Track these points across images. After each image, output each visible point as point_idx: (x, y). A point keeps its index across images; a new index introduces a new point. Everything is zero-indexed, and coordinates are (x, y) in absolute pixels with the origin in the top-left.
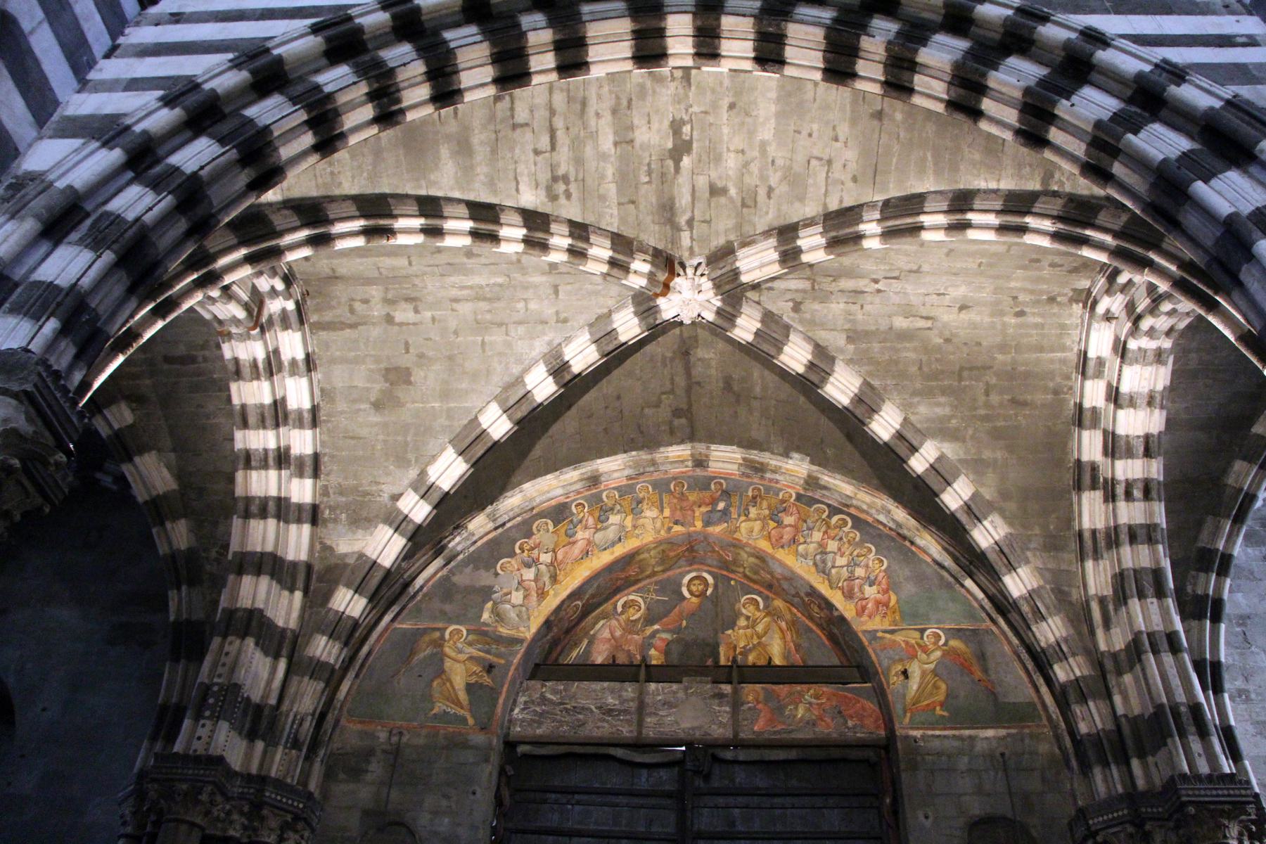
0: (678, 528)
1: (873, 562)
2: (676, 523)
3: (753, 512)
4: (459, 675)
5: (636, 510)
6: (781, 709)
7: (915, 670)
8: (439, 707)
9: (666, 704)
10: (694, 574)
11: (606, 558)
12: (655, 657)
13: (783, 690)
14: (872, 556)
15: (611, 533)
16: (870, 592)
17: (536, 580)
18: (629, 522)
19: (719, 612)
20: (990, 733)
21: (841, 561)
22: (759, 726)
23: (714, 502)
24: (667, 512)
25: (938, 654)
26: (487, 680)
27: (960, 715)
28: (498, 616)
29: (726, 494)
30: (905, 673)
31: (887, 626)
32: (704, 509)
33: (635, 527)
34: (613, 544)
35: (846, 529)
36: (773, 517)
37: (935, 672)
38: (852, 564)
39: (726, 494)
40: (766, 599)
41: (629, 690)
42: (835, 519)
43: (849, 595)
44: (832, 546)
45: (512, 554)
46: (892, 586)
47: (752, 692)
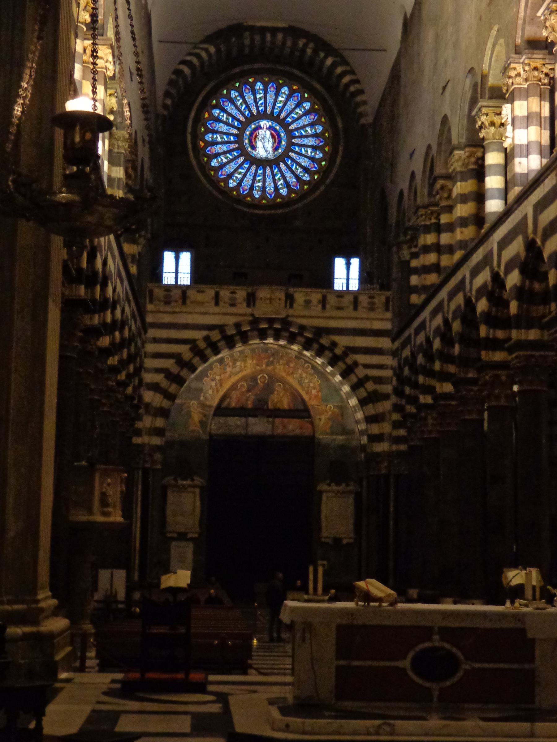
0: (258, 368)
1: (316, 381)
2: (258, 365)
3: (281, 362)
4: (196, 417)
5: (245, 361)
6: (285, 427)
7: (323, 418)
8: (191, 428)
9: (254, 424)
10: (261, 375)
12: (250, 405)
13: (286, 420)
14: (316, 379)
15: (237, 369)
16: (314, 392)
17: (216, 386)
18: (243, 365)
19: (269, 388)
20: (340, 437)
21: (306, 381)
22: (279, 431)
23: (269, 358)
24: (255, 362)
25: (330, 413)
26: (204, 419)
28: (206, 398)
29: (273, 355)
30: (320, 419)
31: (317, 404)
32: (266, 360)
33: (245, 367)
34: (238, 373)
35: (309, 369)
36: (287, 364)
37: (329, 419)
38: (310, 382)
39: (273, 355)
40: (283, 384)
41: (243, 420)
42: (306, 365)
43: (307, 393)
44: (304, 375)
45: (207, 376)
46: (320, 390)
47: (278, 421)
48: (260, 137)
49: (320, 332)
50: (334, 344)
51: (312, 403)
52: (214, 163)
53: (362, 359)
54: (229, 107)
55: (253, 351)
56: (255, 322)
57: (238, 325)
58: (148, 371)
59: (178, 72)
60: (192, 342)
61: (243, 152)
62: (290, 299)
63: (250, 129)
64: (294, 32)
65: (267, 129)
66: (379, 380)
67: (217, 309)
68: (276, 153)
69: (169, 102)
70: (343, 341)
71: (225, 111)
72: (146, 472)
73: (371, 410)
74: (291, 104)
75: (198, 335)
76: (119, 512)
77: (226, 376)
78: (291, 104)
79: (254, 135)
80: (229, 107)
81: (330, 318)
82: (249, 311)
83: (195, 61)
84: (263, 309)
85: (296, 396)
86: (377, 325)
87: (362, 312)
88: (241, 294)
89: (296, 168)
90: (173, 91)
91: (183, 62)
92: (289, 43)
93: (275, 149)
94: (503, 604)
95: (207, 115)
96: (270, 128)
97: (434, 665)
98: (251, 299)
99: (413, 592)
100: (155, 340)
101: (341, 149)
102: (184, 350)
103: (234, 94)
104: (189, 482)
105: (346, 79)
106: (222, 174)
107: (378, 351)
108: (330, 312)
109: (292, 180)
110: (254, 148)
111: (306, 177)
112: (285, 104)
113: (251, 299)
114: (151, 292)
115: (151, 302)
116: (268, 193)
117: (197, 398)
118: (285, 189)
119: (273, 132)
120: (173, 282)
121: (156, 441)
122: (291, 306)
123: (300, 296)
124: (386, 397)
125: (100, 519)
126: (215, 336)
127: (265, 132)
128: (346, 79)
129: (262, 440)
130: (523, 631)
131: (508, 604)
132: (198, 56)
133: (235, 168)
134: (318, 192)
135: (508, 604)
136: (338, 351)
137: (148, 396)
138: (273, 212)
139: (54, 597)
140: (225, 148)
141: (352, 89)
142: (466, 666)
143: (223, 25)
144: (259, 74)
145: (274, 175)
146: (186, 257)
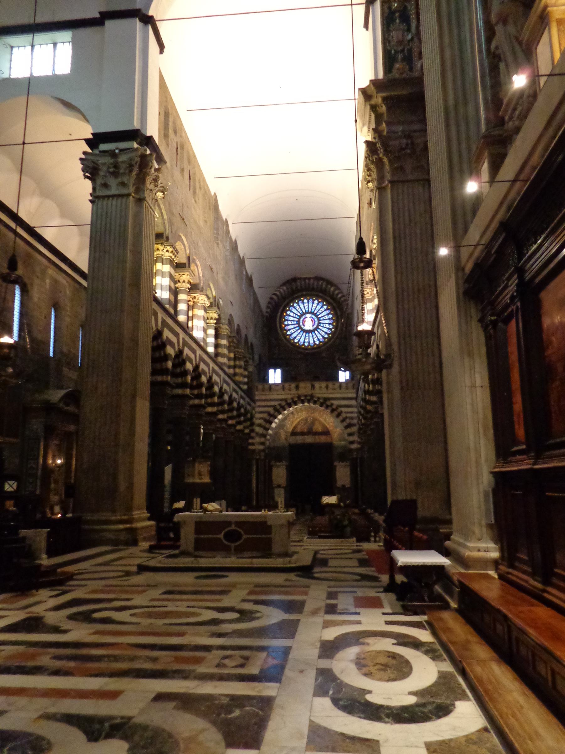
4: (283, 437)
11: (299, 420)
19: (313, 423)
27: (340, 440)
28: (287, 429)
47: (317, 437)
49: (326, 399)
50: (332, 404)
51: (331, 429)
52: (289, 333)
53: (343, 409)
54: (294, 310)
55: (305, 408)
56: (299, 397)
57: (292, 399)
58: (257, 419)
59: (271, 298)
60: (274, 407)
61: (300, 328)
62: (313, 387)
64: (318, 278)
66: (352, 418)
67: (283, 392)
69: (269, 310)
70: (336, 403)
71: (292, 312)
72: (257, 460)
73: (349, 430)
74: (319, 307)
75: (276, 403)
76: (208, 478)
77: (293, 418)
78: (319, 307)
80: (294, 310)
81: (330, 393)
82: (296, 392)
83: (278, 293)
84: (302, 391)
85: (324, 426)
86: (350, 395)
87: (343, 390)
88: (293, 385)
90: (270, 306)
91: (275, 294)
92: (316, 283)
94: (261, 511)
95: (285, 314)
96: (311, 317)
97: (232, 536)
98: (297, 387)
99: (244, 508)
100: (259, 406)
102: (271, 410)
103: (295, 305)
104: (281, 463)
105: (339, 296)
106: (292, 337)
107: (350, 406)
108: (330, 391)
109: (320, 338)
110: (304, 326)
111: (326, 336)
113: (297, 387)
114: (257, 387)
115: (257, 391)
117: (283, 429)
120: (273, 382)
121: (261, 447)
122: (314, 389)
123: (317, 385)
124: (354, 425)
125: (197, 481)
126: (283, 403)
128: (339, 296)
129: (310, 445)
130: (265, 522)
131: (263, 511)
132: (280, 292)
135: (263, 511)
136: (334, 407)
137: (257, 429)
139: (148, 513)
140: (292, 327)
141: (342, 299)
142: (245, 537)
143: (287, 278)
144: (305, 296)
145: (313, 336)
146: (279, 371)
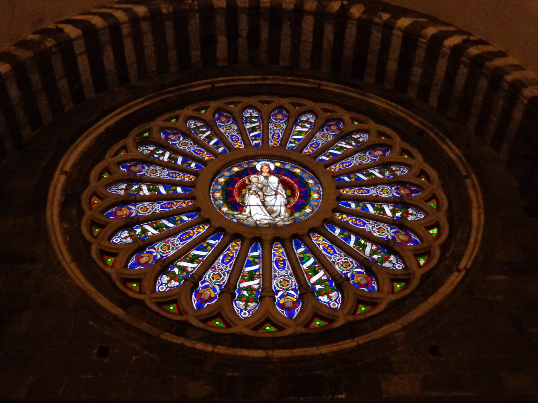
48: (254, 188)
63: (227, 174)
65: (271, 173)
68: (297, 215)
79: (238, 184)
89: (357, 242)
93: (294, 208)
101: (475, 196)
110: (239, 207)
112: (311, 136)
116: (282, 306)
118: (334, 295)
119: (286, 178)
127: (266, 178)
133: (181, 246)
134: (445, 290)
138: (299, 352)
